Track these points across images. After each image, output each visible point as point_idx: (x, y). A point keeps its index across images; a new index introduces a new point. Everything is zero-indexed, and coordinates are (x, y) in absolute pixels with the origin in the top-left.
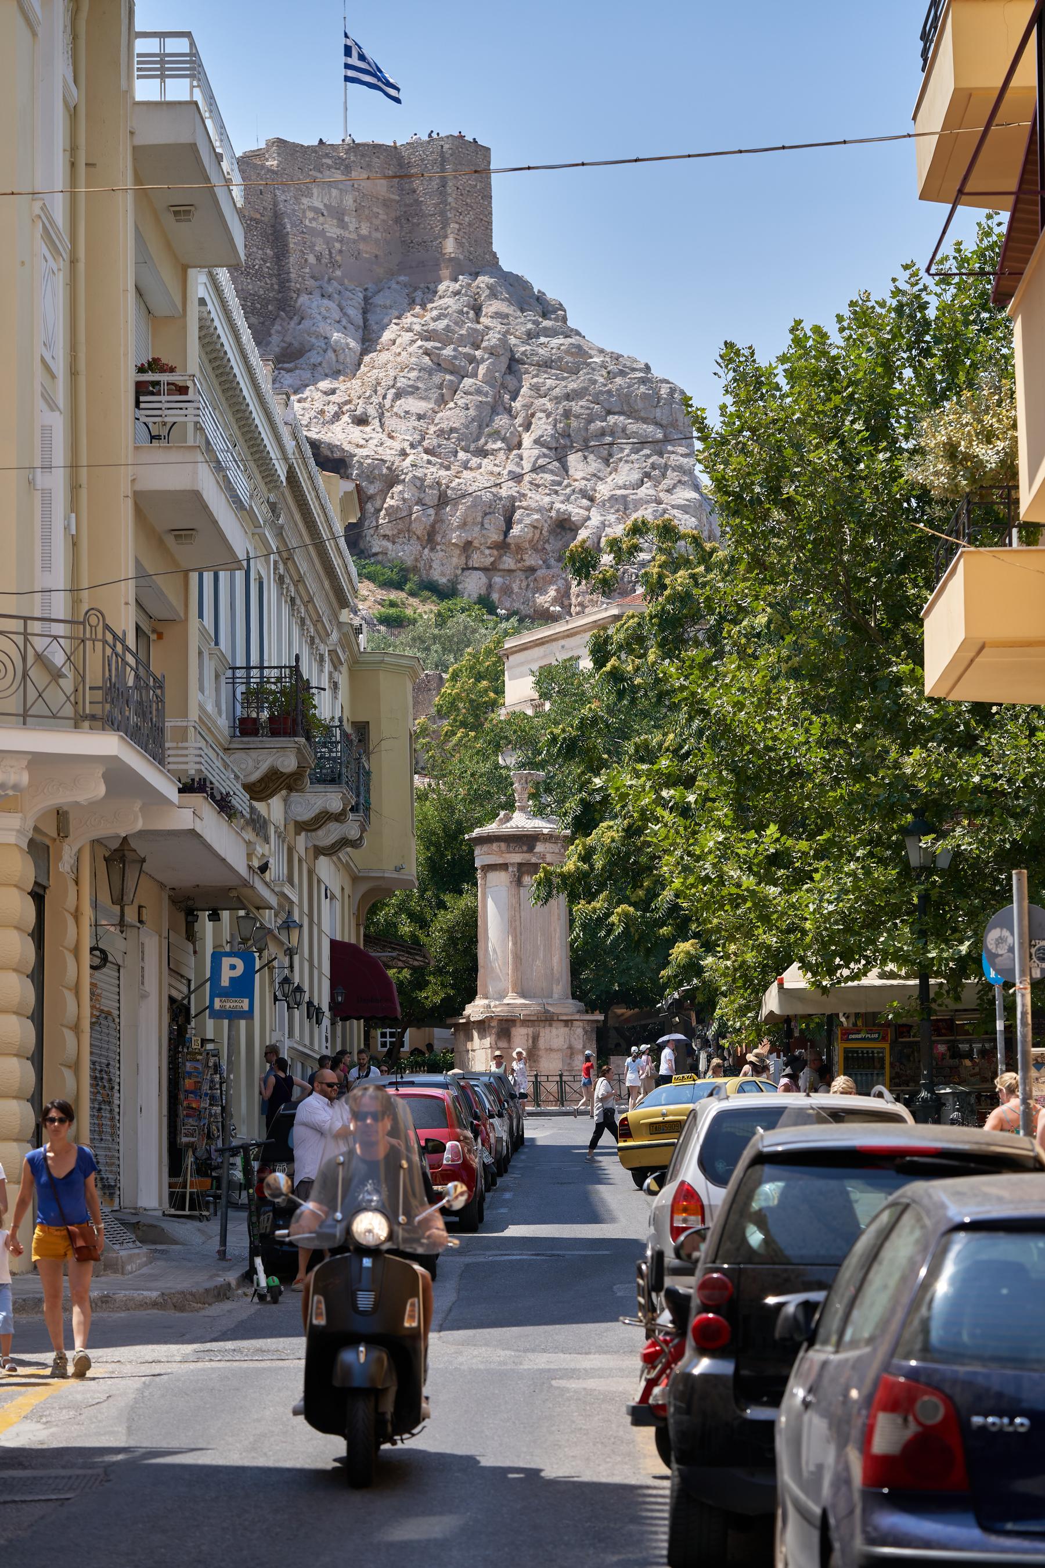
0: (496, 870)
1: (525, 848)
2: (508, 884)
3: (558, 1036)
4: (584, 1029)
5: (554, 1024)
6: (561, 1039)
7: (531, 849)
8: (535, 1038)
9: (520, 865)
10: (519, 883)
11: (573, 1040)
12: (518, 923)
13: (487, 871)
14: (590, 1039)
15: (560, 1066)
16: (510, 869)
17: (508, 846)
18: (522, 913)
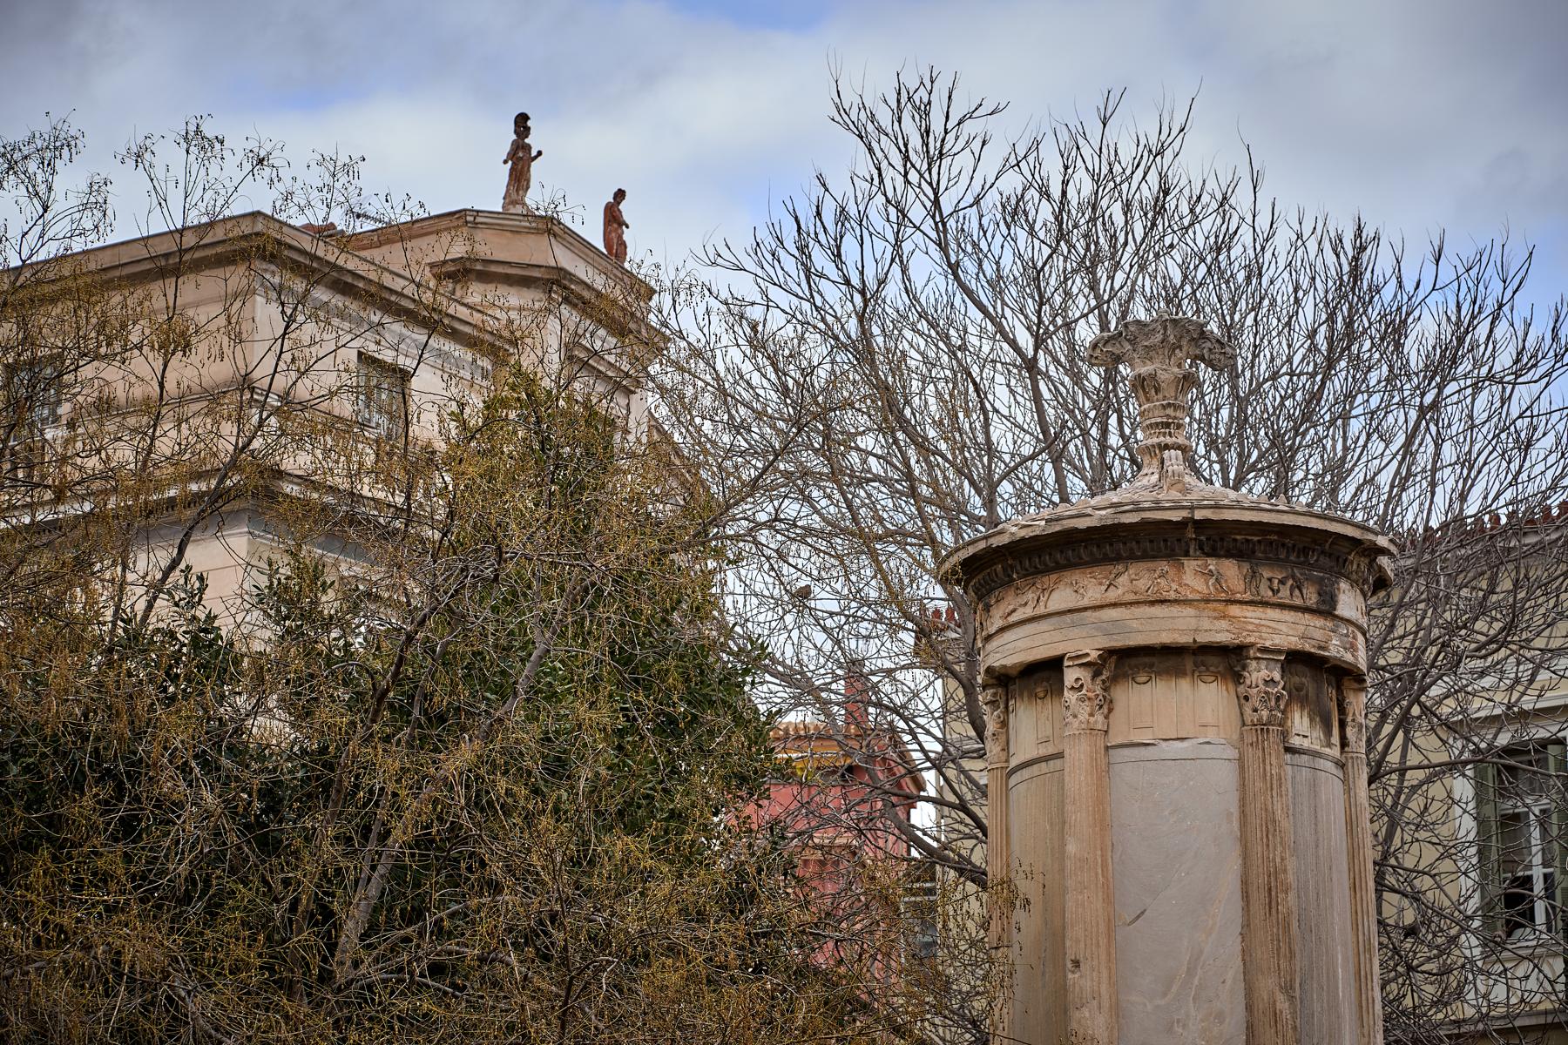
0: (1179, 673)
1: (1311, 596)
9: (1295, 660)
13: (1114, 679)
16: (1259, 673)
17: (1255, 574)
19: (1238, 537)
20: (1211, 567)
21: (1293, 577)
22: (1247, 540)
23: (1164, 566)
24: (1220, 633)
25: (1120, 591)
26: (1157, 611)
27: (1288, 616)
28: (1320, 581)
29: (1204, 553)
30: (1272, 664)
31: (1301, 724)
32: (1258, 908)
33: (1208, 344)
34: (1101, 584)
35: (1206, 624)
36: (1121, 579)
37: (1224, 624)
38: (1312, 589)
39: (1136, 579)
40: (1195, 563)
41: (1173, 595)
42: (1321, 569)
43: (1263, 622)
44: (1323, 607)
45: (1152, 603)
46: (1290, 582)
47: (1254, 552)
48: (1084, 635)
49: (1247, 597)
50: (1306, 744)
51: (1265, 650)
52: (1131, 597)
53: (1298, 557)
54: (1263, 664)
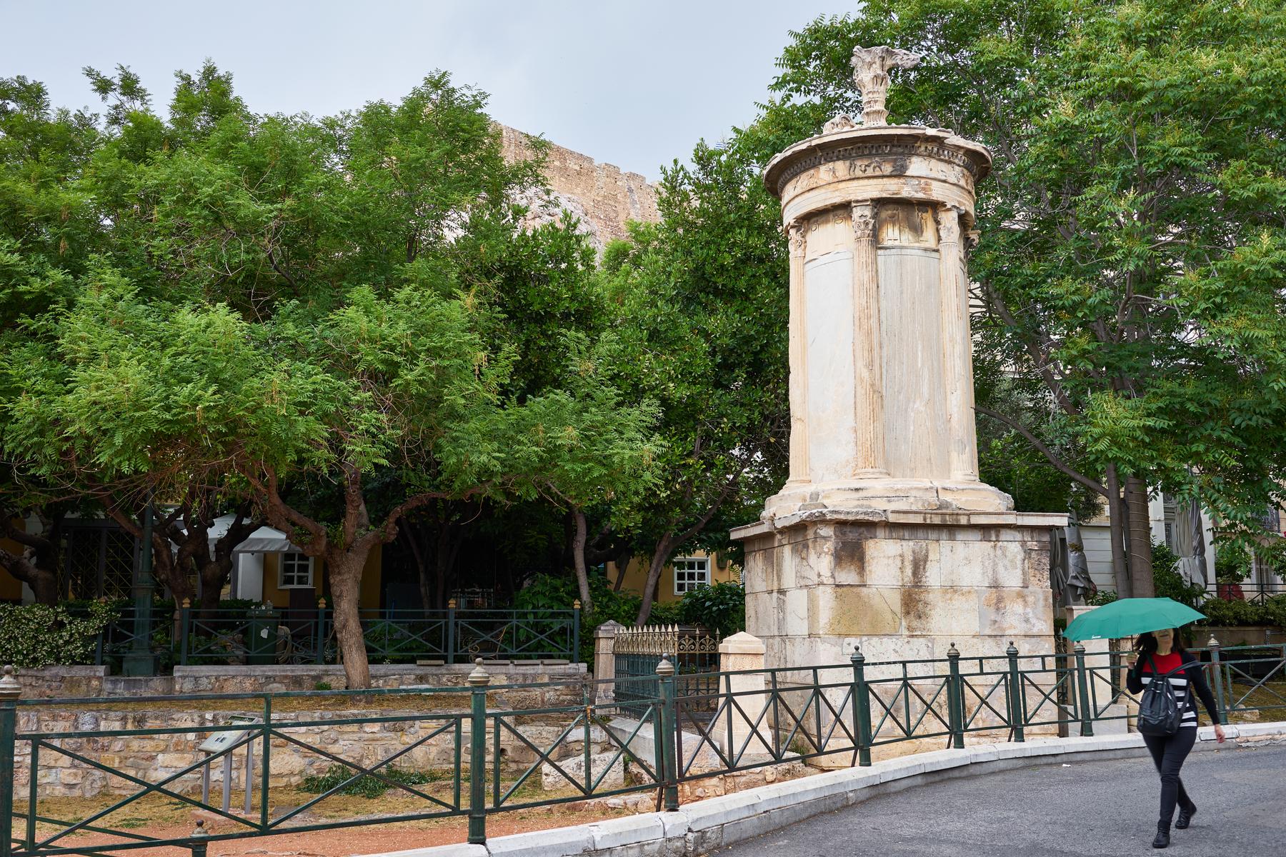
0: (827, 222)
2: (852, 244)
3: (968, 560)
4: (1023, 543)
5: (961, 536)
6: (978, 570)
7: (899, 173)
8: (919, 565)
9: (879, 203)
10: (875, 240)
11: (1001, 569)
12: (874, 321)
13: (806, 231)
14: (1037, 567)
15: (975, 627)
16: (857, 212)
18: (883, 304)
23: (812, 172)
24: (837, 199)
26: (812, 193)
27: (871, 181)
28: (895, 161)
31: (891, 234)
32: (857, 329)
33: (900, 57)
35: (829, 195)
37: (837, 193)
39: (803, 181)
41: (815, 186)
42: (895, 154)
44: (894, 173)
45: (809, 190)
49: (848, 177)
50: (897, 243)
51: (857, 201)
52: (800, 191)
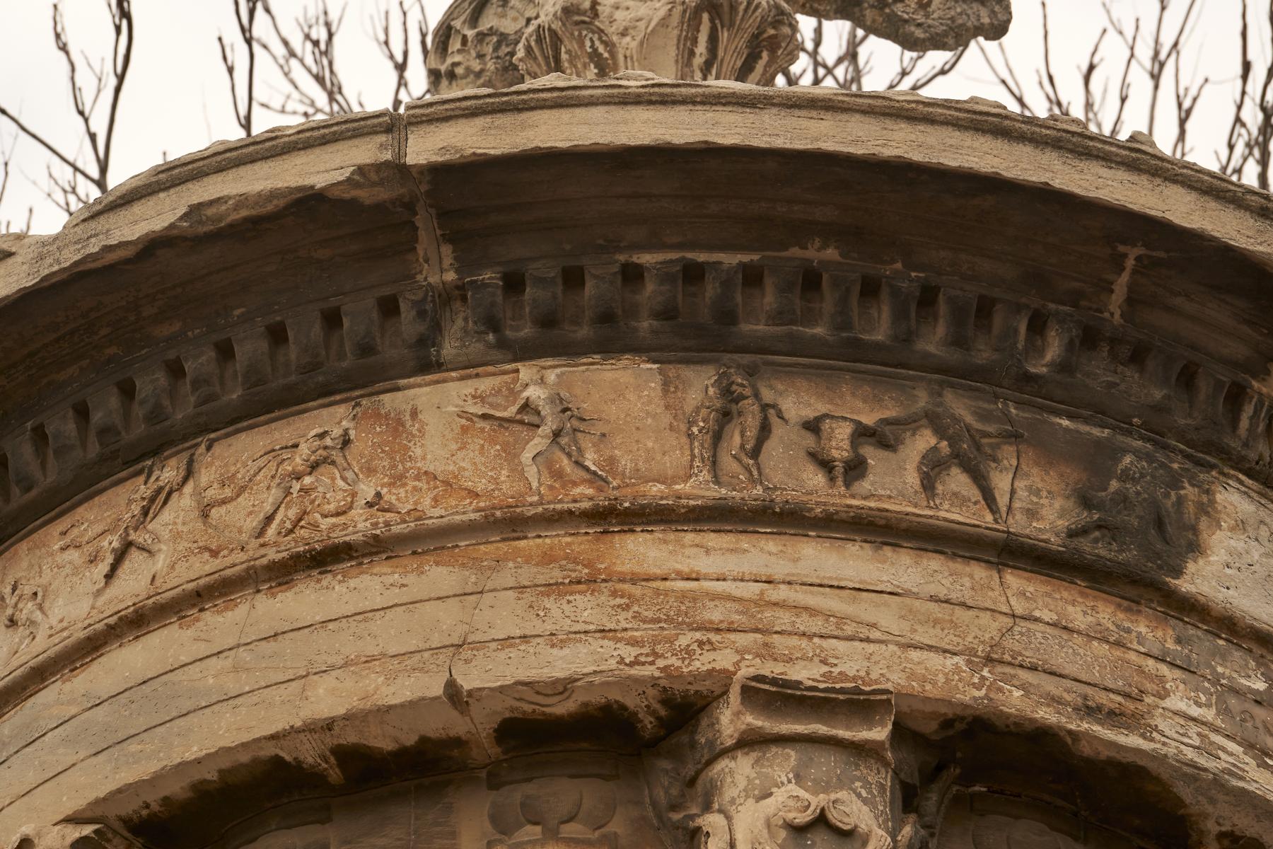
19: (646, 258)
20: (535, 393)
21: (936, 421)
22: (693, 274)
25: (161, 562)
29: (502, 344)
30: (826, 764)
34: (93, 560)
36: (167, 515)
38: (1036, 477)
40: (468, 387)
41: (360, 525)
42: (1097, 411)
43: (782, 593)
44: (1097, 549)
46: (923, 441)
47: (727, 317)
48: (32, 778)
53: (958, 341)
54: (783, 763)
